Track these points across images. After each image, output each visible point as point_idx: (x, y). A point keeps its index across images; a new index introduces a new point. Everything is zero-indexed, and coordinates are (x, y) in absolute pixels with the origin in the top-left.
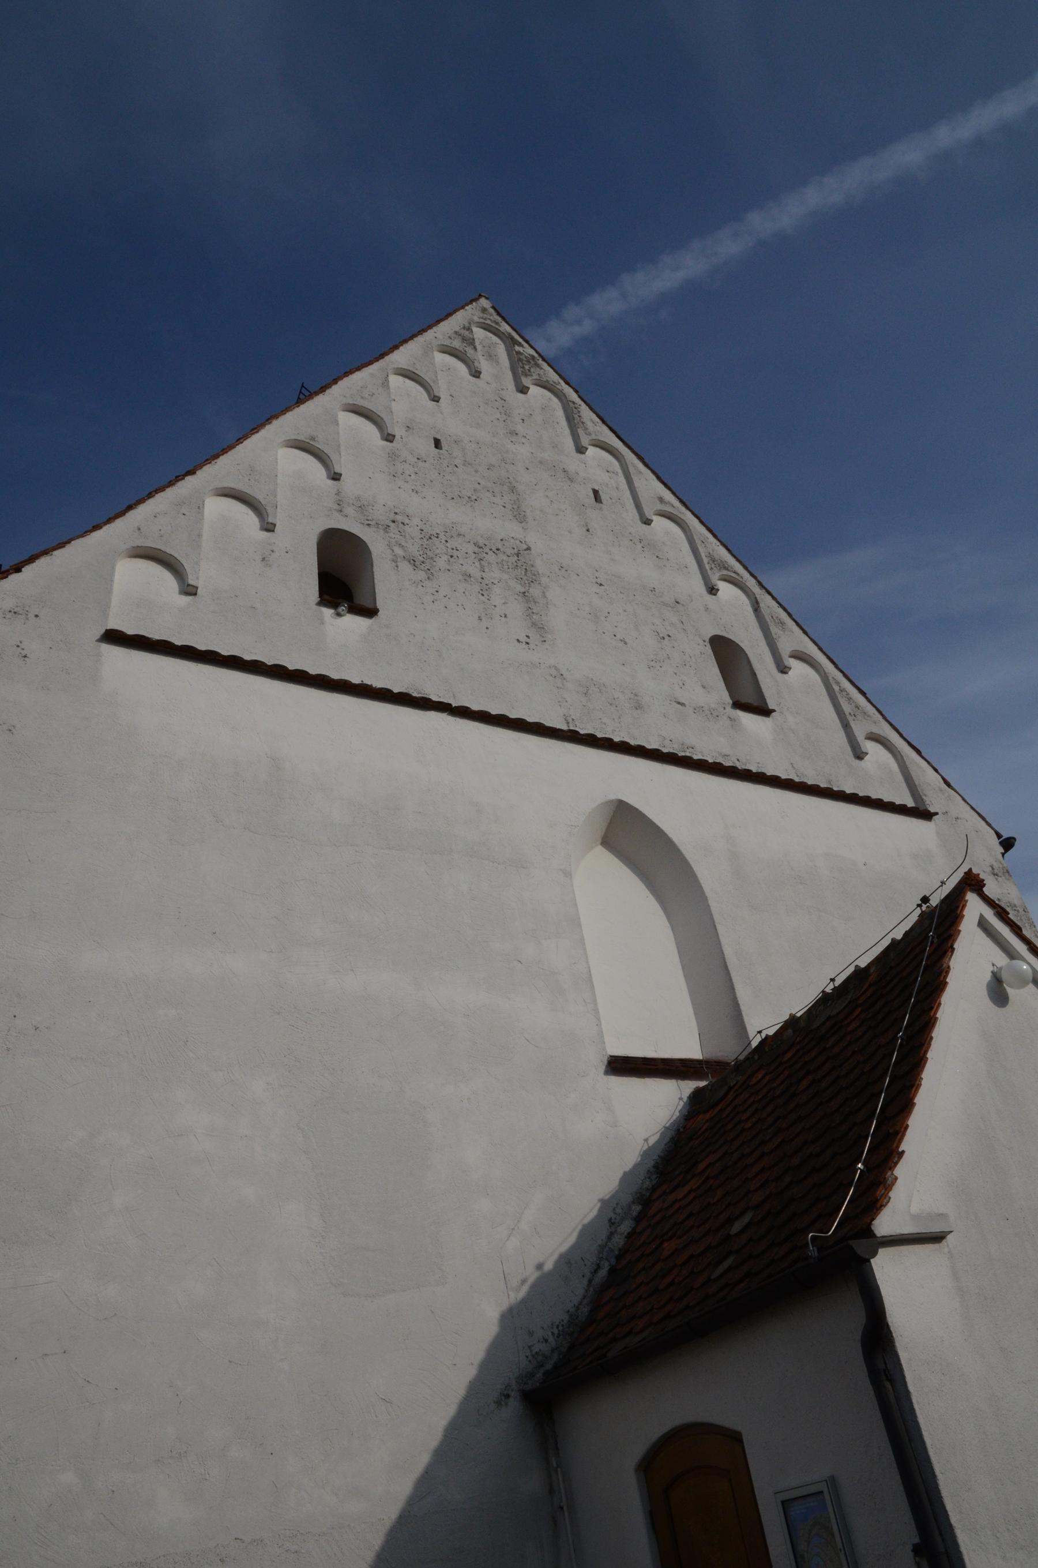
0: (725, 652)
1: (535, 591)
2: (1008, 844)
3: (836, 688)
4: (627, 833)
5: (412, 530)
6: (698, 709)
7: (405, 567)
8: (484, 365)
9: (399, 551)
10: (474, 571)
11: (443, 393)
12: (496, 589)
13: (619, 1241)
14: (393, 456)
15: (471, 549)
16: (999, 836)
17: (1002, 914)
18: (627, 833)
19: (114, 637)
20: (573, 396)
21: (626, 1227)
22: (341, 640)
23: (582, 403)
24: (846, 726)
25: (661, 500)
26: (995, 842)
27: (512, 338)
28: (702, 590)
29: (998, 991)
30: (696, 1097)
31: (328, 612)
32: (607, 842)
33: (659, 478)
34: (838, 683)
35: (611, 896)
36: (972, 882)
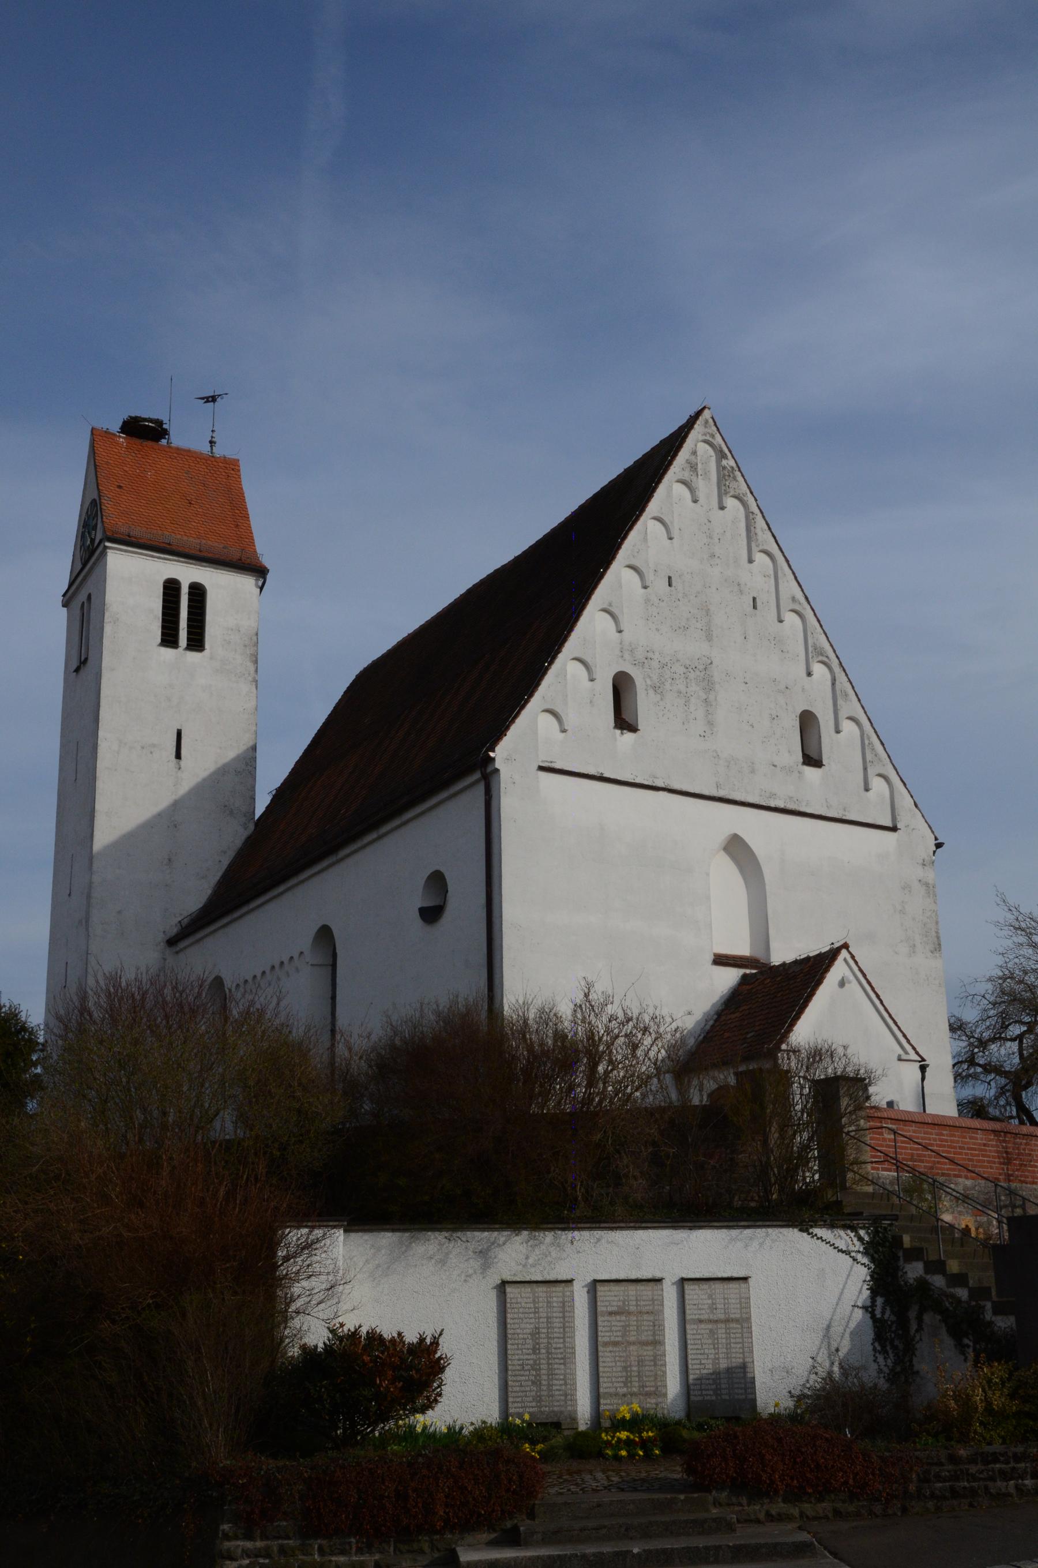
0: (807, 721)
1: (712, 697)
2: (939, 846)
3: (867, 742)
4: (736, 848)
5: (655, 664)
6: (783, 768)
7: (651, 692)
8: (701, 495)
9: (649, 682)
10: (682, 688)
11: (675, 533)
12: (693, 700)
13: (708, 1027)
14: (647, 601)
15: (682, 670)
16: (936, 839)
17: (853, 957)
18: (736, 848)
19: (541, 768)
20: (756, 511)
21: (711, 1023)
22: (622, 752)
23: (760, 515)
24: (865, 769)
25: (794, 599)
26: (932, 843)
27: (721, 451)
28: (804, 673)
29: (842, 984)
30: (745, 977)
31: (618, 732)
32: (726, 849)
33: (796, 578)
34: (869, 738)
35: (725, 874)
36: (846, 946)
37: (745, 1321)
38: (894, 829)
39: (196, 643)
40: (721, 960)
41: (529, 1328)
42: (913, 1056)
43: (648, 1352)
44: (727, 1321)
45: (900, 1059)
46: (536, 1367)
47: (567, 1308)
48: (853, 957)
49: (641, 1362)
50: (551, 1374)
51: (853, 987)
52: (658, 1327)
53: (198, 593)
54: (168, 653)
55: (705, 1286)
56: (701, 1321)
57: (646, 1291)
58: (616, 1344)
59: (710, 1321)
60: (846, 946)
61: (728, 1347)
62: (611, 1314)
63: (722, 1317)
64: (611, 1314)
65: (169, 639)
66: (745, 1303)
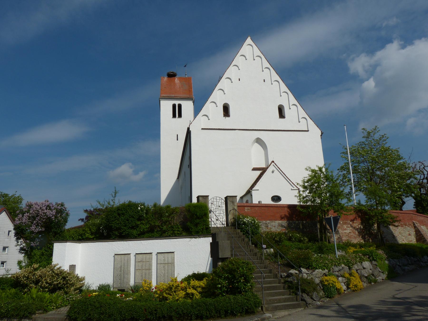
2: (322, 133)
4: (259, 141)
17: (276, 164)
18: (259, 141)
19: (202, 129)
22: (227, 122)
29: (273, 172)
36: (273, 162)
37: (173, 264)
38: (308, 131)
39: (180, 116)
40: (254, 169)
41: (119, 266)
42: (295, 188)
43: (147, 271)
44: (168, 263)
45: (292, 190)
46: (120, 275)
47: (129, 261)
48: (276, 164)
49: (145, 274)
50: (124, 277)
51: (276, 171)
52: (151, 265)
53: (180, 106)
54: (174, 119)
55: (163, 254)
56: (161, 264)
57: (148, 256)
58: (140, 270)
59: (163, 264)
60: (273, 162)
61: (168, 270)
62: (139, 262)
63: (167, 262)
64: (139, 262)
65: (174, 116)
66: (173, 259)
